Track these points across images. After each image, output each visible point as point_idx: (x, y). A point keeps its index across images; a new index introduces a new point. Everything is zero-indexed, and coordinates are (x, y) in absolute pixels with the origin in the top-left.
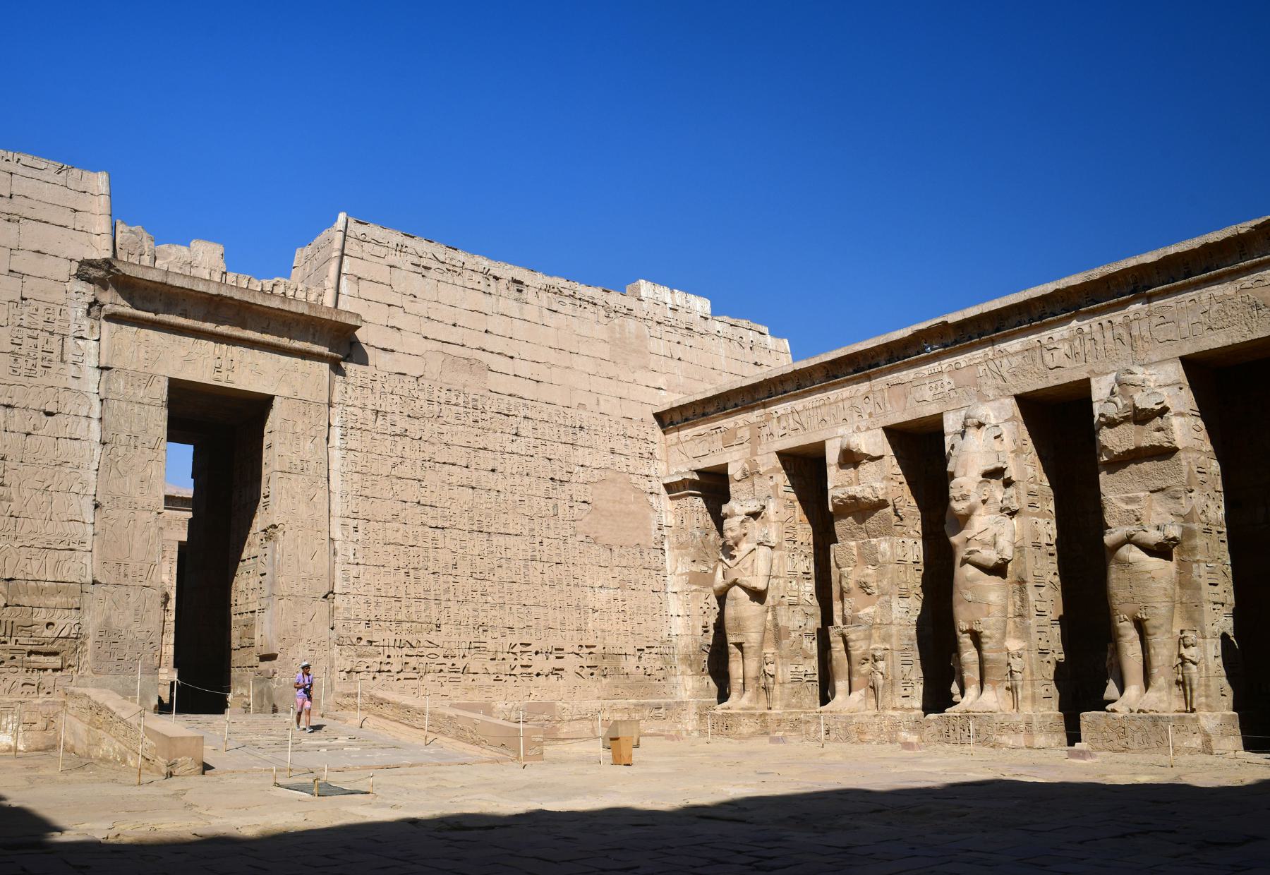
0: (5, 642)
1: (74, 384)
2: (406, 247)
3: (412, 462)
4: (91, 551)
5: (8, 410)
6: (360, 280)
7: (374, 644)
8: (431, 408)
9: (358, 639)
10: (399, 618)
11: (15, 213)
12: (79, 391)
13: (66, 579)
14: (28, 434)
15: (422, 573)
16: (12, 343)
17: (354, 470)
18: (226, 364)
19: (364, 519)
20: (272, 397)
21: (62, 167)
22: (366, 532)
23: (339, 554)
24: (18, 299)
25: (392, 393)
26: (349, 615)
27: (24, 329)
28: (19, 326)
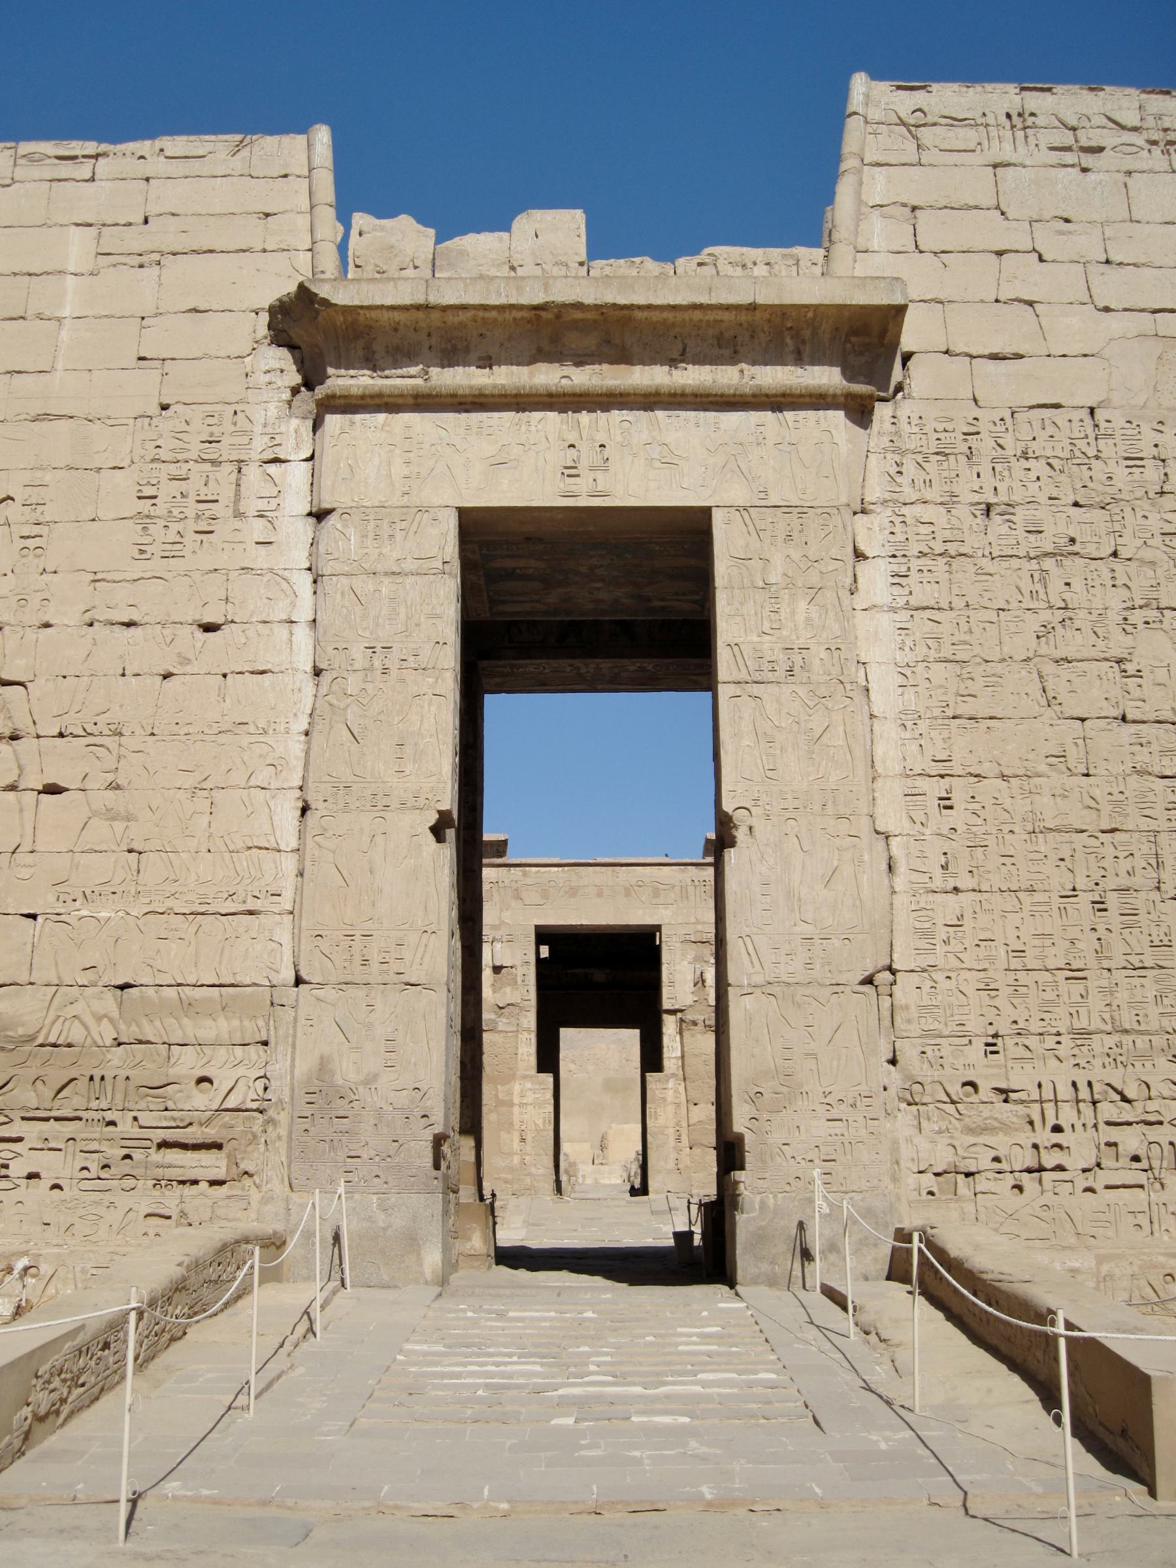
0: (112, 1123)
1: (261, 558)
2: (1032, 114)
3: (1094, 617)
4: (291, 913)
5: (133, 628)
6: (918, 212)
7: (1010, 1094)
8: (1137, 476)
9: (965, 1084)
10: (1084, 1023)
11: (152, 249)
12: (271, 570)
13: (239, 979)
14: (165, 677)
15: (1139, 901)
16: (139, 498)
17: (933, 655)
18: (587, 456)
19: (971, 775)
20: (706, 512)
21: (241, 142)
22: (976, 806)
23: (901, 867)
24: (154, 410)
25: (1025, 456)
26: (936, 1025)
27: (163, 466)
28: (153, 461)
